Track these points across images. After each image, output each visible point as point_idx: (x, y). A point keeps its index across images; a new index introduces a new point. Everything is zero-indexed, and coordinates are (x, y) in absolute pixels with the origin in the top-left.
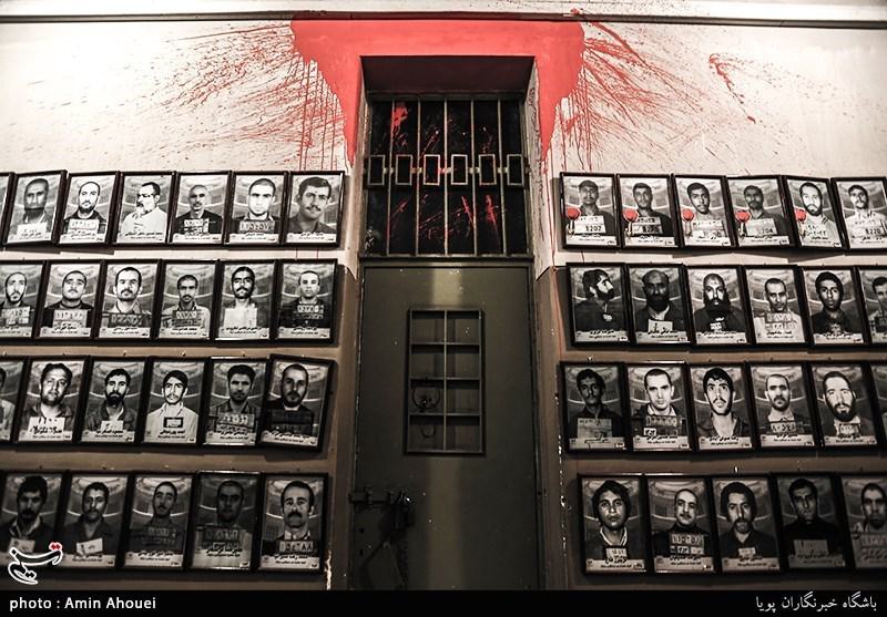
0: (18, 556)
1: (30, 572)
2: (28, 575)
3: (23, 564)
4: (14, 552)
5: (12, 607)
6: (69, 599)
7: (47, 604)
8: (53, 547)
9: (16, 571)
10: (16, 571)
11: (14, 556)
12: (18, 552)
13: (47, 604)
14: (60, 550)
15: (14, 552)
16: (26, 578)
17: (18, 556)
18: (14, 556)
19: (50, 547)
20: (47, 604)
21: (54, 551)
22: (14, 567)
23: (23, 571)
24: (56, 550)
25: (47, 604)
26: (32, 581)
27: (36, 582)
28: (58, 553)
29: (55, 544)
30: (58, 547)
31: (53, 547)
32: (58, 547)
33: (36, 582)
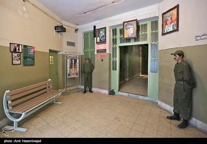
0: (4, 130)
2: (6, 134)
3: (6, 132)
4: (3, 129)
5: (4, 142)
6: (15, 140)
7: (11, 141)
8: (12, 128)
9: (4, 133)
10: (4, 133)
11: (3, 130)
15: (3, 129)
16: (5, 135)
17: (4, 130)
18: (3, 130)
20: (11, 141)
22: (3, 132)
23: (5, 133)
24: (13, 128)
26: (7, 136)
30: (14, 128)
31: (12, 128)
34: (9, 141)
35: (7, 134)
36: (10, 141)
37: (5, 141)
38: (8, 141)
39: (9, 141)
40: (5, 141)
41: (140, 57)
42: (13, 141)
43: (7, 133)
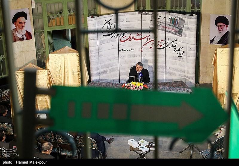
0: (5, 150)
2: (7, 155)
4: (3, 149)
5: (3, 163)
7: (11, 163)
8: (14, 147)
9: (4, 154)
10: (4, 154)
12: (4, 148)
13: (10, 162)
14: (16, 148)
16: (6, 155)
19: (13, 147)
20: (11, 163)
21: (14, 148)
23: (6, 154)
24: (15, 148)
26: (9, 156)
27: (9, 157)
28: (15, 149)
29: (15, 146)
30: (15, 147)
31: (14, 147)
32: (15, 147)
33: (9, 157)
34: (8, 163)
35: (8, 155)
36: (10, 162)
37: (4, 163)
38: (7, 163)
39: (8, 163)
40: (4, 163)
42: (13, 163)
43: (8, 153)
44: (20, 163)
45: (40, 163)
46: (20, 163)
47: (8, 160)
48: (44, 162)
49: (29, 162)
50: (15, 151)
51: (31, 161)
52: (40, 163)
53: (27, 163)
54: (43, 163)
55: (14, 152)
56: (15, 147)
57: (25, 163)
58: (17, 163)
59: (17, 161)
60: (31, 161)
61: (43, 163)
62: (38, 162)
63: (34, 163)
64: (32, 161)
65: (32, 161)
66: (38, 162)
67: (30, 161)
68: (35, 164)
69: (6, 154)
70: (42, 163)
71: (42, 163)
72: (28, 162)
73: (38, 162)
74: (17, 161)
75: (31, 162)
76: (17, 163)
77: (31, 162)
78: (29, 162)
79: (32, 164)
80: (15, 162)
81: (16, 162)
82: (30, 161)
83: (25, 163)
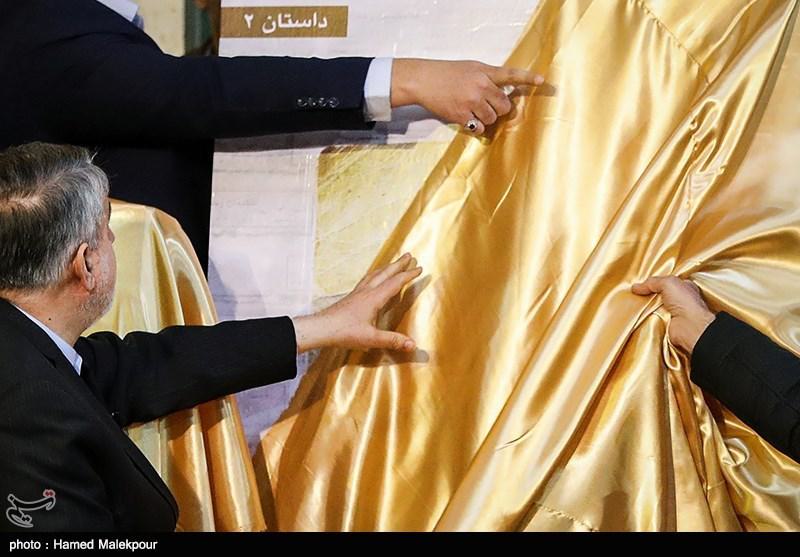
0: (15, 502)
1: (25, 517)
2: (24, 519)
4: (11, 498)
5: (11, 548)
7: (37, 545)
8: (47, 494)
10: (13, 516)
11: (12, 502)
13: (34, 545)
15: (11, 498)
16: (21, 521)
17: (15, 502)
19: (44, 494)
20: (37, 545)
21: (47, 497)
22: (11, 512)
23: (20, 515)
24: (49, 496)
25: (34, 545)
26: (28, 524)
27: (32, 526)
28: (51, 500)
29: (49, 491)
31: (47, 494)
32: (51, 494)
33: (32, 526)
34: (27, 545)
35: (28, 519)
37: (14, 545)
38: (23, 546)
39: (27, 545)
40: (14, 545)
41: (486, 126)
42: (43, 546)
43: (25, 513)
44: (66, 545)
45: (135, 545)
46: (66, 545)
47: (25, 535)
48: (146, 545)
49: (96, 544)
50: (49, 506)
51: (103, 542)
52: (135, 545)
53: (90, 545)
54: (142, 545)
55: (47, 509)
56: (49, 493)
57: (83, 545)
58: (58, 546)
59: (58, 541)
60: (103, 542)
61: (142, 545)
62: (126, 545)
63: (113, 546)
64: (107, 541)
65: (107, 541)
66: (126, 545)
67: (100, 541)
68: (118, 552)
69: (20, 515)
70: (139, 545)
71: (139, 545)
72: (92, 542)
73: (128, 545)
74: (58, 541)
75: (103, 545)
76: (58, 546)
77: (103, 545)
78: (96, 544)
79: (107, 551)
80: (52, 544)
81: (55, 544)
82: (100, 541)
83: (83, 545)
